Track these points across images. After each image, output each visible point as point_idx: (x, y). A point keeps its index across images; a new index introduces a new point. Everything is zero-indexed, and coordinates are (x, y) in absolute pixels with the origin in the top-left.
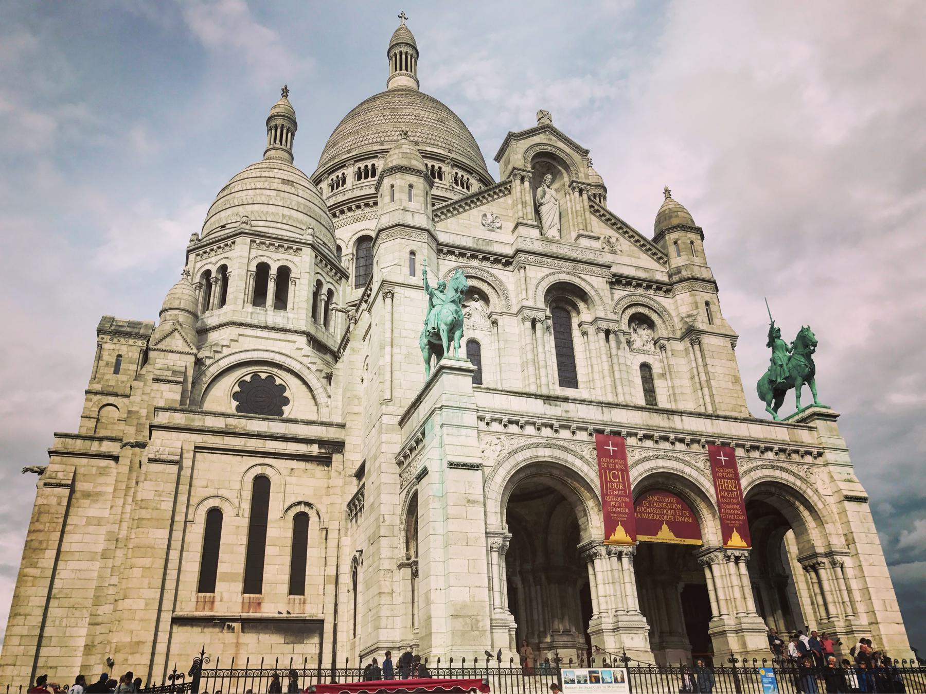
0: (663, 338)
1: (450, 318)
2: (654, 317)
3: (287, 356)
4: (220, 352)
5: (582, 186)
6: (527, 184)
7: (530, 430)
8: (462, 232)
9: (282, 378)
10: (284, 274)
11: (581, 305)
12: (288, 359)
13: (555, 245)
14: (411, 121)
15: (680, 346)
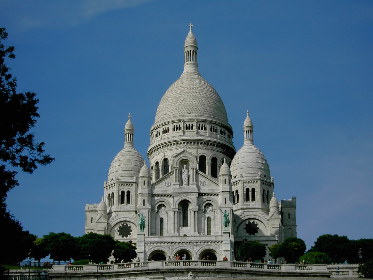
0: (214, 209)
1: (140, 224)
2: (212, 203)
3: (130, 218)
4: (114, 220)
5: (194, 168)
6: (177, 171)
7: (155, 244)
8: (159, 189)
9: (129, 225)
10: (129, 192)
11: (190, 204)
12: (131, 219)
13: (182, 189)
14: (182, 103)
15: (219, 211)
